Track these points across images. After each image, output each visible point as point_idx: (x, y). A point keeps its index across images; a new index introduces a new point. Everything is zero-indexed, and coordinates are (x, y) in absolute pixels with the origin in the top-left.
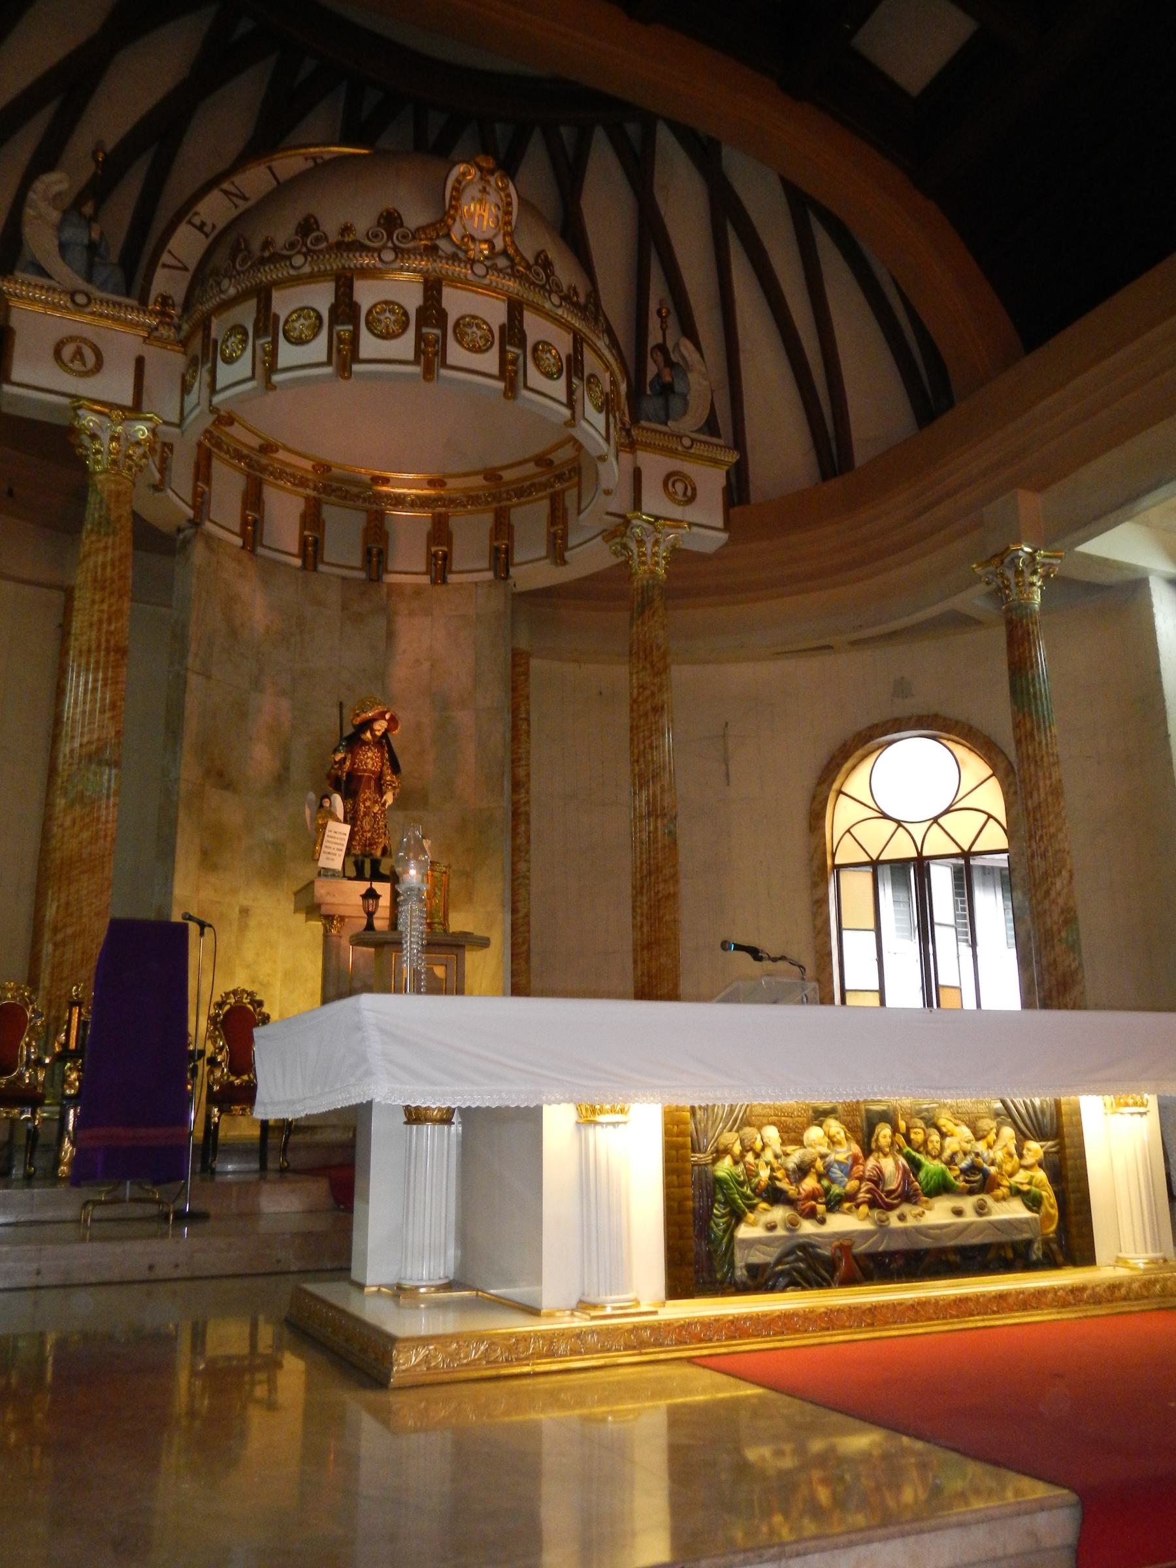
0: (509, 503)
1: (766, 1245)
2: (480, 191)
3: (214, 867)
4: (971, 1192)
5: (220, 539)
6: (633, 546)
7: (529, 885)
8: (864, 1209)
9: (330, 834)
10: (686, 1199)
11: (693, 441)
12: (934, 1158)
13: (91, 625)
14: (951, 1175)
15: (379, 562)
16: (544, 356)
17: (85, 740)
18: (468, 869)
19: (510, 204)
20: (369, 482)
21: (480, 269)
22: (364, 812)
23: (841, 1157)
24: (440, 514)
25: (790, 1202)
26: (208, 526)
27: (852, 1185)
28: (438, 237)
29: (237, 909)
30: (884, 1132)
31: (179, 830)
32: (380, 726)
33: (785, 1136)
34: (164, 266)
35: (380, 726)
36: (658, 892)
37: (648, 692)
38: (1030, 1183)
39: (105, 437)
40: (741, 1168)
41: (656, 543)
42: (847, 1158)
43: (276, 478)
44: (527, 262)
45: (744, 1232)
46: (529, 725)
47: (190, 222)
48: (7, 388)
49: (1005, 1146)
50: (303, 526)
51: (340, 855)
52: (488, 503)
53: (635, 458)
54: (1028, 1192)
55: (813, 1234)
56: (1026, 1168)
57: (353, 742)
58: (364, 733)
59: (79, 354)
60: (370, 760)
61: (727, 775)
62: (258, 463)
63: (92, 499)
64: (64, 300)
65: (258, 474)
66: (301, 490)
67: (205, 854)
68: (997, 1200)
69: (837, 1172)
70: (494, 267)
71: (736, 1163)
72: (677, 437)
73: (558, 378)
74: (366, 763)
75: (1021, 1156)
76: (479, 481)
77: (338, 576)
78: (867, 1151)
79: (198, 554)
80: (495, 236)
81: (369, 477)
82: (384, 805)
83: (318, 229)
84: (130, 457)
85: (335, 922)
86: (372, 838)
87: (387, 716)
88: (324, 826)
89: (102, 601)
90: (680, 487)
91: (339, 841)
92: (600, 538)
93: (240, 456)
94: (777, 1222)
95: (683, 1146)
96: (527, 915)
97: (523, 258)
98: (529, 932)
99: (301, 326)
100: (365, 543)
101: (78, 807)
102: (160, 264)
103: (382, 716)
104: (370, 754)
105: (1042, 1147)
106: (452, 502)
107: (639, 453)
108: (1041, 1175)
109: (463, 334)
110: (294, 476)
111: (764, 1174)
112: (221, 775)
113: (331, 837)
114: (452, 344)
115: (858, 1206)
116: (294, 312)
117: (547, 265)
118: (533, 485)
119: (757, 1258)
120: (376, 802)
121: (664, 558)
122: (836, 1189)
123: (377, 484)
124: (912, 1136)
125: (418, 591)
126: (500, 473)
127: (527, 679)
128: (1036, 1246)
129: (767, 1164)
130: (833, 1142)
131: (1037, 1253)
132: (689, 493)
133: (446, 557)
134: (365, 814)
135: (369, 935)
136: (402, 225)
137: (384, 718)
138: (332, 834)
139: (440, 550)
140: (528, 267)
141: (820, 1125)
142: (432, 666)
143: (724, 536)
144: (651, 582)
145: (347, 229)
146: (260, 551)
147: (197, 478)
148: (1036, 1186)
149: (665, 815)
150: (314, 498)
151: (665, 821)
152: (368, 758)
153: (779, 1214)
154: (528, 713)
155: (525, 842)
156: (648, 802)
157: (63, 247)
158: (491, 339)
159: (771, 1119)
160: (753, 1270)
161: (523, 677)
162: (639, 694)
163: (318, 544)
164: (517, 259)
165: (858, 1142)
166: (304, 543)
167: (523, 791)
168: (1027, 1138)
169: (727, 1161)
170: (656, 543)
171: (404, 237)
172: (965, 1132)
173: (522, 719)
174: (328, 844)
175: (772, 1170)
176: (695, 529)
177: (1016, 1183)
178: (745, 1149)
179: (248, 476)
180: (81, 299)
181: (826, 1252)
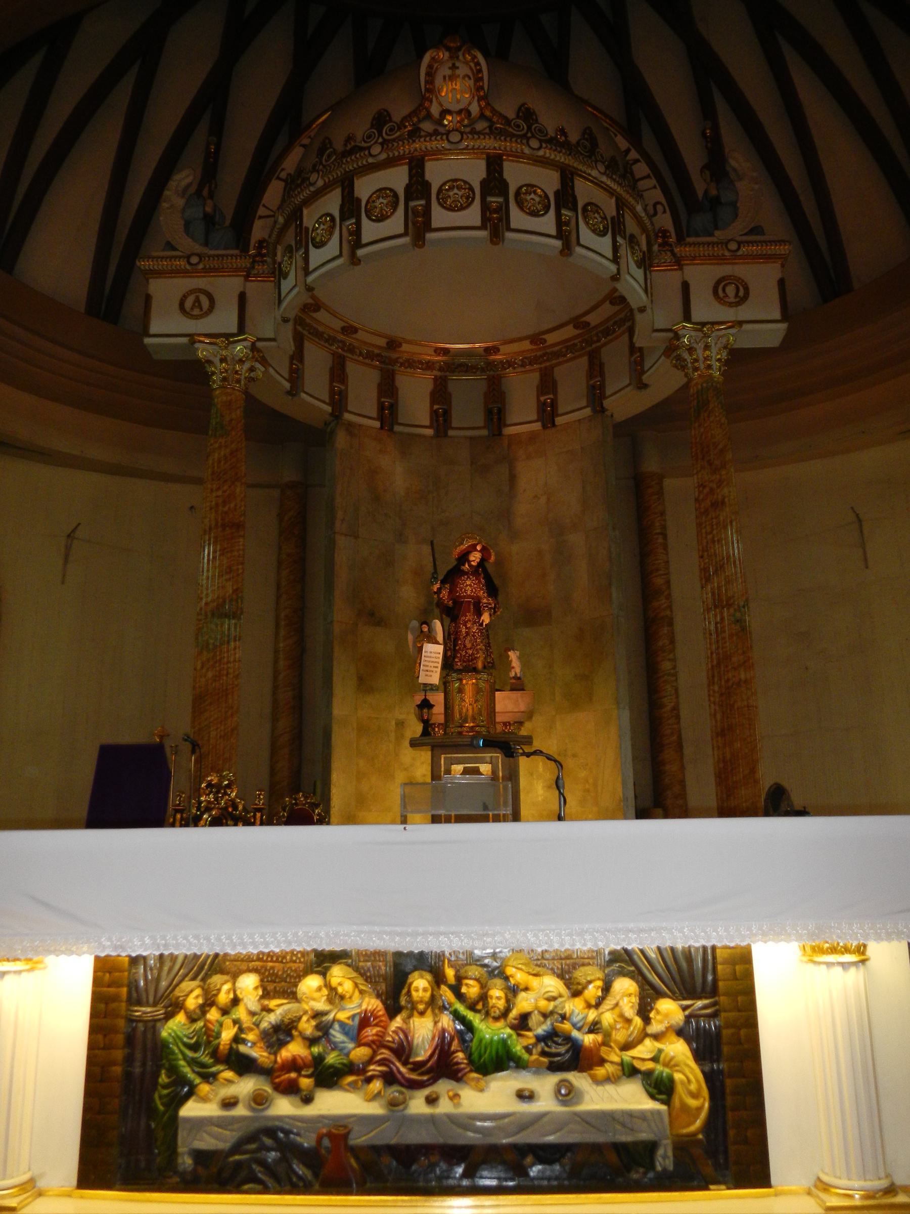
0: (598, 344)
1: (218, 1126)
2: (450, 68)
3: (370, 690)
4: (554, 1068)
5: (360, 425)
6: (686, 355)
8: (377, 1085)
9: (426, 654)
10: (114, 1063)
11: (739, 244)
12: (496, 1019)
13: (211, 509)
14: (518, 1048)
16: (528, 198)
17: (209, 599)
19: (480, 71)
20: (483, 353)
21: (455, 137)
22: (466, 632)
23: (342, 1016)
24: (546, 368)
25: (266, 1072)
26: (347, 416)
27: (360, 1053)
28: (420, 121)
29: (393, 722)
30: (420, 984)
31: (335, 663)
32: (475, 557)
33: (270, 987)
34: (260, 217)
35: (475, 557)
36: (728, 680)
37: (706, 490)
38: (655, 1059)
39: (216, 361)
40: (200, 1024)
41: (707, 347)
42: (353, 1017)
43: (406, 368)
44: (505, 118)
45: (190, 1110)
47: (278, 178)
48: (147, 341)
49: (617, 1005)
51: (436, 672)
52: (583, 348)
53: (683, 273)
54: (648, 1074)
55: (289, 1117)
56: (657, 1037)
57: (453, 575)
58: (464, 565)
59: (197, 300)
60: (470, 587)
61: (866, 560)
63: (213, 411)
64: (182, 263)
66: (429, 372)
67: (361, 679)
68: (597, 1082)
69: (337, 1035)
70: (473, 132)
71: (192, 1020)
72: (722, 243)
73: (546, 213)
74: (465, 590)
75: (647, 1020)
76: (569, 332)
77: (466, 438)
78: (393, 1010)
79: (341, 439)
80: (470, 104)
81: (482, 349)
82: (481, 625)
83: (331, 147)
84: (236, 372)
85: (437, 729)
86: (473, 654)
87: (479, 548)
88: (421, 649)
89: (218, 489)
90: (731, 290)
92: (663, 357)
93: (370, 356)
94: (241, 1097)
95: (115, 998)
97: (501, 116)
99: (321, 230)
101: (205, 653)
102: (257, 217)
103: (473, 548)
104: (468, 582)
105: (684, 1008)
106: (556, 355)
107: (685, 267)
108: (678, 1049)
109: (445, 199)
110: (420, 362)
111: (227, 1035)
112: (372, 614)
113: (427, 657)
114: (436, 210)
115: (369, 1080)
116: (316, 222)
117: (527, 114)
118: (615, 323)
119: (206, 1142)
120: (475, 623)
121: (719, 360)
122: (332, 1058)
123: (491, 354)
124: (464, 990)
125: (532, 437)
126: (584, 319)
128: (660, 1152)
129: (236, 1022)
130: (335, 997)
131: (664, 1159)
132: (741, 293)
133: (554, 404)
134: (467, 634)
135: (426, 740)
136: (390, 120)
137: (476, 550)
138: (429, 654)
139: (547, 398)
140: (508, 122)
141: (324, 974)
142: (548, 499)
143: (783, 326)
144: (705, 385)
145: (349, 139)
147: (332, 381)
148: (666, 1065)
149: (729, 606)
150: (441, 377)
151: (732, 610)
152: (467, 585)
153: (246, 1086)
154: (664, 527)
156: (713, 594)
157: (187, 224)
158: (471, 196)
159: (252, 965)
160: (200, 1156)
161: (655, 497)
162: (700, 492)
163: (447, 413)
164: (495, 119)
165: (378, 996)
166: (434, 414)
168: (660, 994)
169: (181, 1018)
170: (707, 347)
171: (391, 130)
172: (551, 984)
174: (427, 663)
175: (241, 1030)
176: (746, 327)
177: (634, 1058)
178: (209, 1002)
180: (194, 260)
181: (307, 1142)
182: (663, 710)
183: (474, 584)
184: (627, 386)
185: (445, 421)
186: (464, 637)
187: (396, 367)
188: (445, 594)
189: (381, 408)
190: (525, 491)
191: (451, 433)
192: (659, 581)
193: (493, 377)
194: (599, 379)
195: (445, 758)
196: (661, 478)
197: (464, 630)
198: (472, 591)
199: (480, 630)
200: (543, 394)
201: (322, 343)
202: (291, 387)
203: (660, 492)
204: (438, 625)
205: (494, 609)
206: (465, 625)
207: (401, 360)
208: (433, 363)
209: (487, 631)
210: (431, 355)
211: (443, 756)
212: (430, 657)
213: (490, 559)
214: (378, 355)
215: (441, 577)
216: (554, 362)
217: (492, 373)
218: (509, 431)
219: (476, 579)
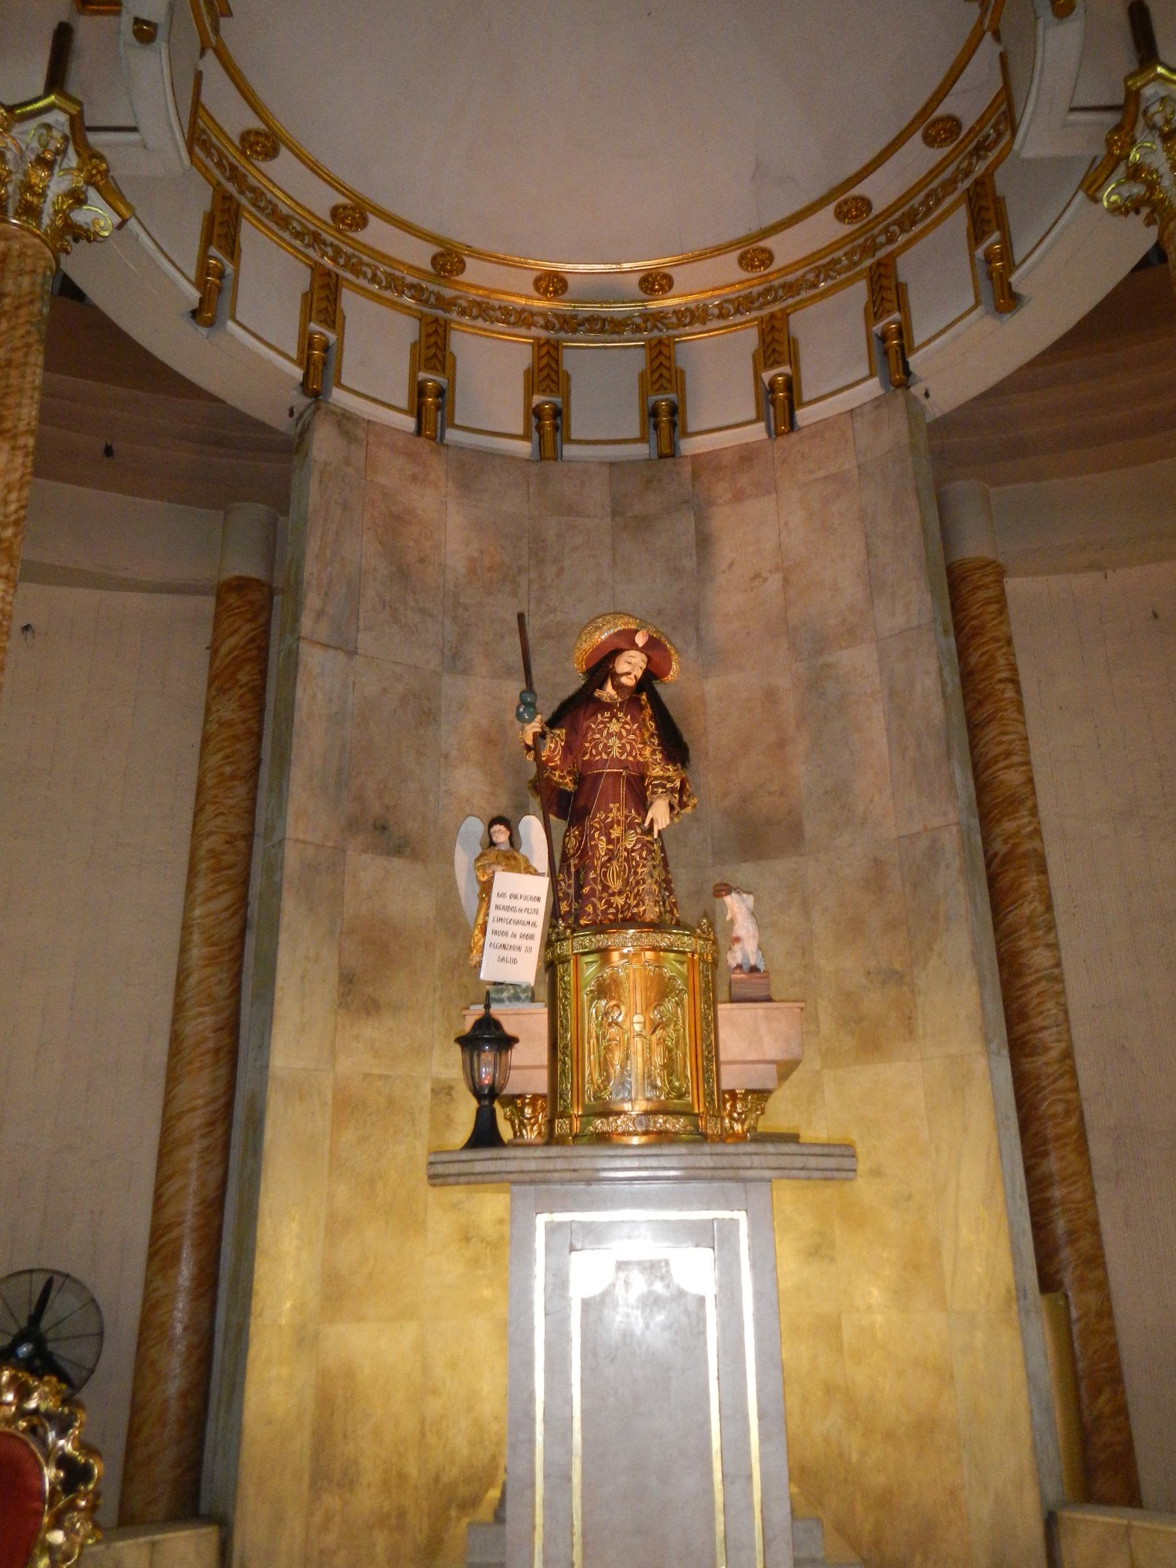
3: (372, 1007)
15: (673, 424)
18: (897, 966)
24: (772, 316)
26: (338, 396)
29: (427, 1088)
31: (283, 937)
32: (631, 665)
35: (631, 665)
46: (1018, 691)
50: (531, 387)
51: (529, 950)
58: (601, 686)
62: (439, 297)
65: (440, 313)
66: (523, 331)
67: (348, 980)
81: (636, 278)
85: (528, 1111)
87: (640, 640)
88: (486, 888)
91: (524, 917)
93: (394, 283)
96: (1068, 1055)
98: (1076, 1088)
100: (643, 397)
104: (614, 727)
106: (791, 288)
110: (506, 311)
112: (382, 828)
113: (507, 908)
120: (630, 826)
125: (747, 456)
127: (1003, 609)
133: (791, 385)
134: (611, 856)
137: (634, 646)
142: (786, 580)
146: (452, 435)
147: (306, 317)
150: (548, 341)
152: (610, 735)
154: (1013, 668)
155: (1041, 908)
161: (993, 608)
167: (1024, 812)
173: (1001, 681)
174: (501, 927)
179: (421, 318)
182: (1040, 1060)
183: (629, 732)
186: (603, 865)
187: (454, 316)
188: (553, 748)
189: (419, 391)
190: (731, 565)
191: (569, 451)
192: (1012, 778)
193: (660, 342)
194: (896, 316)
195: (552, 1229)
196: (1000, 573)
197: (602, 845)
198: (623, 747)
199: (647, 845)
200: (768, 366)
201: (286, 235)
202: (201, 300)
203: (1001, 600)
204: (533, 829)
205: (682, 790)
206: (606, 829)
207: (464, 303)
208: (532, 314)
209: (663, 849)
210: (528, 297)
212: (513, 909)
213: (670, 668)
214: (412, 287)
215: (548, 706)
216: (791, 301)
217: (656, 333)
218: (690, 446)
219: (634, 720)
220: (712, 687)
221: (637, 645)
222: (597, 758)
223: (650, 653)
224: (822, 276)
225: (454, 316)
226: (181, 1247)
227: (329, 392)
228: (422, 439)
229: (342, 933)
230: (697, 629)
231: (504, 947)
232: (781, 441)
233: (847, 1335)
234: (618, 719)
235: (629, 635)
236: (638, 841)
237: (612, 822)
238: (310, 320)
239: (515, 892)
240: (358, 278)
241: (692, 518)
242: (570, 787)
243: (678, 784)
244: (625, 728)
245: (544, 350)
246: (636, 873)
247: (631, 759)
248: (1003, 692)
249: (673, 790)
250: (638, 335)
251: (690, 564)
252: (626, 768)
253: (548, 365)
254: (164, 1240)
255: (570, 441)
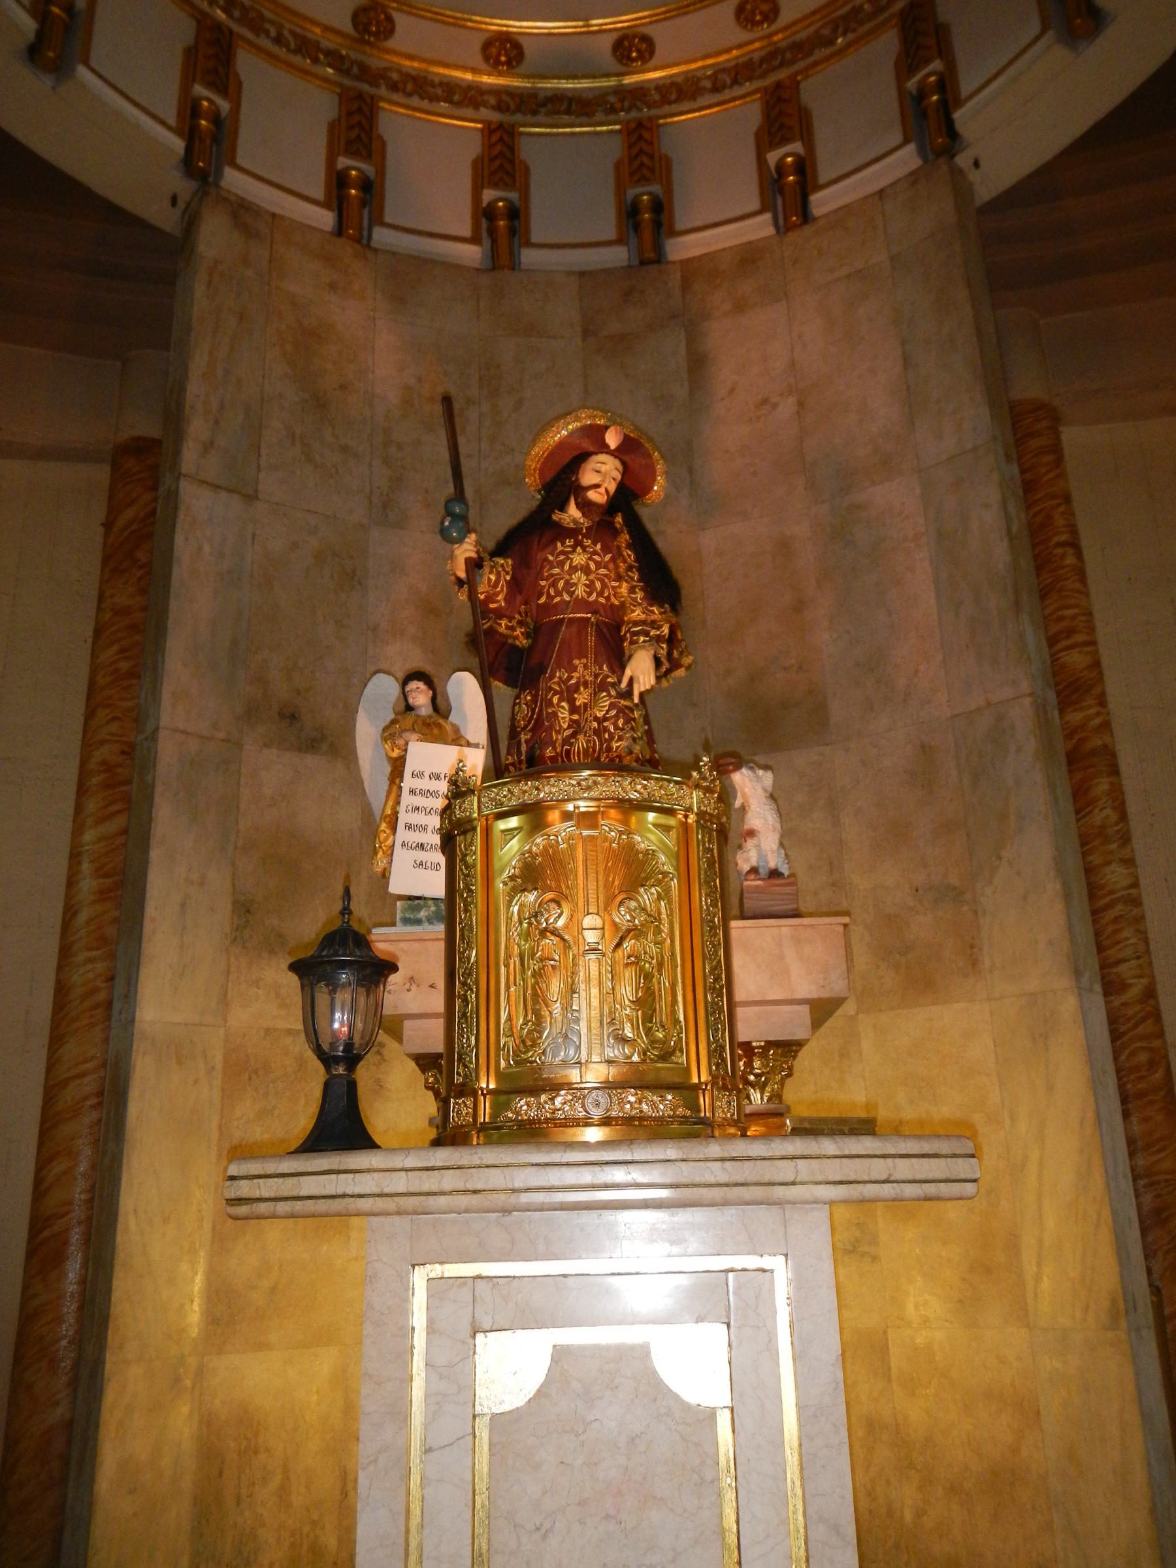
5: (274, 215)
7: (1141, 919)
18: (954, 880)
24: (778, 85)
26: (232, 179)
31: (155, 854)
58: (563, 508)
65: (366, 87)
66: (469, 112)
81: (608, 42)
82: (628, 694)
87: (612, 439)
88: (398, 767)
96: (1150, 993)
98: (1161, 1034)
100: (620, 191)
104: (579, 559)
106: (800, 49)
112: (290, 716)
120: (603, 687)
127: (1059, 461)
133: (804, 167)
137: (603, 448)
142: (801, 404)
146: (381, 236)
150: (501, 126)
152: (573, 569)
154: (1073, 530)
155: (1114, 816)
161: (1046, 459)
167: (1090, 701)
183: (598, 565)
184: (1037, 39)
185: (512, 231)
186: (566, 741)
189: (338, 182)
190: (732, 390)
191: (529, 257)
193: (640, 125)
196: (1055, 420)
197: (564, 714)
198: (590, 586)
199: (621, 711)
200: (774, 144)
205: (672, 640)
206: (569, 695)
207: (395, 76)
210: (474, 71)
211: (420, 1278)
213: (654, 480)
214: (328, 53)
217: (634, 114)
218: (682, 248)
220: (709, 541)
221: (608, 446)
222: (557, 599)
223: (627, 458)
224: (840, 30)
225: (383, 91)
226: (66, 1243)
227: (219, 173)
228: (343, 240)
229: (236, 848)
230: (691, 471)
231: (422, 846)
232: (792, 236)
233: (897, 1359)
234: (584, 549)
235: (596, 434)
236: (612, 706)
237: (578, 684)
238: (194, 81)
239: (436, 771)
240: (258, 35)
241: (683, 336)
242: (523, 642)
243: (666, 630)
244: (594, 561)
245: (495, 138)
246: (609, 749)
247: (602, 600)
248: (1063, 556)
249: (658, 639)
250: (612, 117)
251: (680, 391)
252: (594, 612)
253: (501, 154)
254: (46, 1233)
255: (529, 244)
